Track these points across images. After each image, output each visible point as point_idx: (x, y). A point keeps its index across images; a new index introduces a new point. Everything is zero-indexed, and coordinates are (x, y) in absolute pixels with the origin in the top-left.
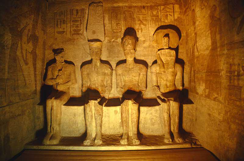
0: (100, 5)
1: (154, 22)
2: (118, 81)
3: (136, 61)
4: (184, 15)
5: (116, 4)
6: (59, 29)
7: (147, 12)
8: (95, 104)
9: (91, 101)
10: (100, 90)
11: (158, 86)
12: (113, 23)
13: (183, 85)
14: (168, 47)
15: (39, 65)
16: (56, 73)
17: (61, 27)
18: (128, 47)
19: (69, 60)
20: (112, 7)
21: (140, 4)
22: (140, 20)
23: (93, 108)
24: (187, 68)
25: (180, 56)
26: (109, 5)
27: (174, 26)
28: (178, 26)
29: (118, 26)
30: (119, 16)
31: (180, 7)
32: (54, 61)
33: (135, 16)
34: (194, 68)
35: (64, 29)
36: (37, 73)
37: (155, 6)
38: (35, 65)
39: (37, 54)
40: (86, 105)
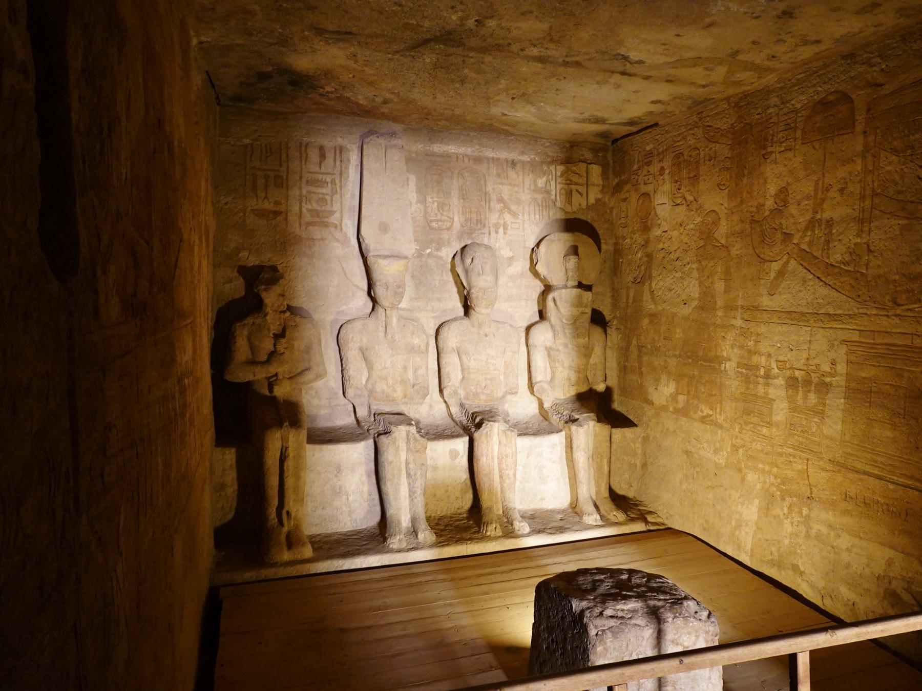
0: (395, 146)
1: (537, 208)
2: (447, 370)
4: (613, 194)
7: (521, 178)
8: (407, 435)
9: (400, 427)
12: (430, 200)
14: (576, 283)
18: (482, 277)
22: (501, 200)
23: (403, 445)
28: (595, 225)
31: (605, 175)
33: (489, 188)
34: (638, 339)
37: (542, 163)
40: (383, 439)
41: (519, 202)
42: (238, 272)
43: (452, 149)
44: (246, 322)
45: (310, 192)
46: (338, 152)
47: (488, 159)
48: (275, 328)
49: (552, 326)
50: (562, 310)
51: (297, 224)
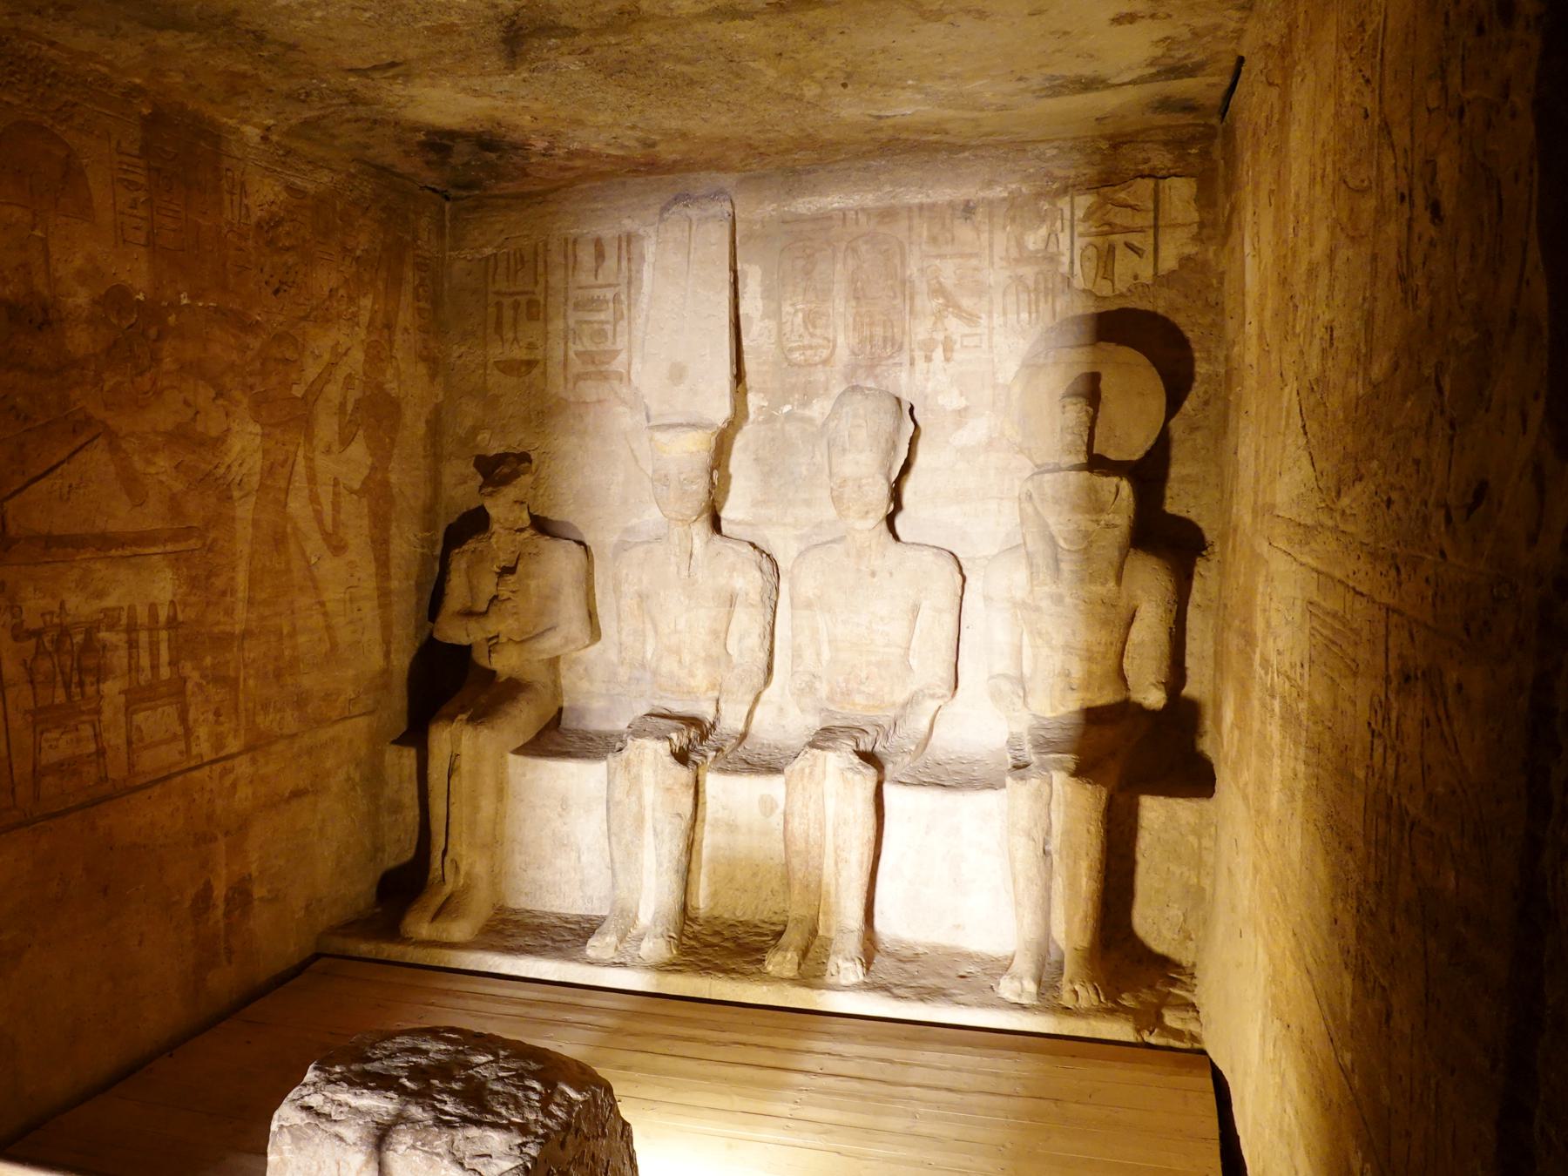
1: (1024, 297)
5: (807, 199)
6: (507, 346)
7: (985, 236)
11: (1021, 681)
12: (791, 310)
15: (406, 543)
16: (488, 586)
17: (516, 339)
20: (788, 218)
22: (939, 291)
27: (1152, 316)
29: (815, 327)
33: (913, 270)
35: (531, 347)
36: (394, 584)
39: (395, 490)
41: (980, 290)
42: (476, 465)
43: (834, 201)
44: (465, 547)
45: (579, 322)
46: (624, 245)
47: (910, 209)
48: (504, 559)
49: (1029, 555)
50: (1051, 520)
51: (561, 381)
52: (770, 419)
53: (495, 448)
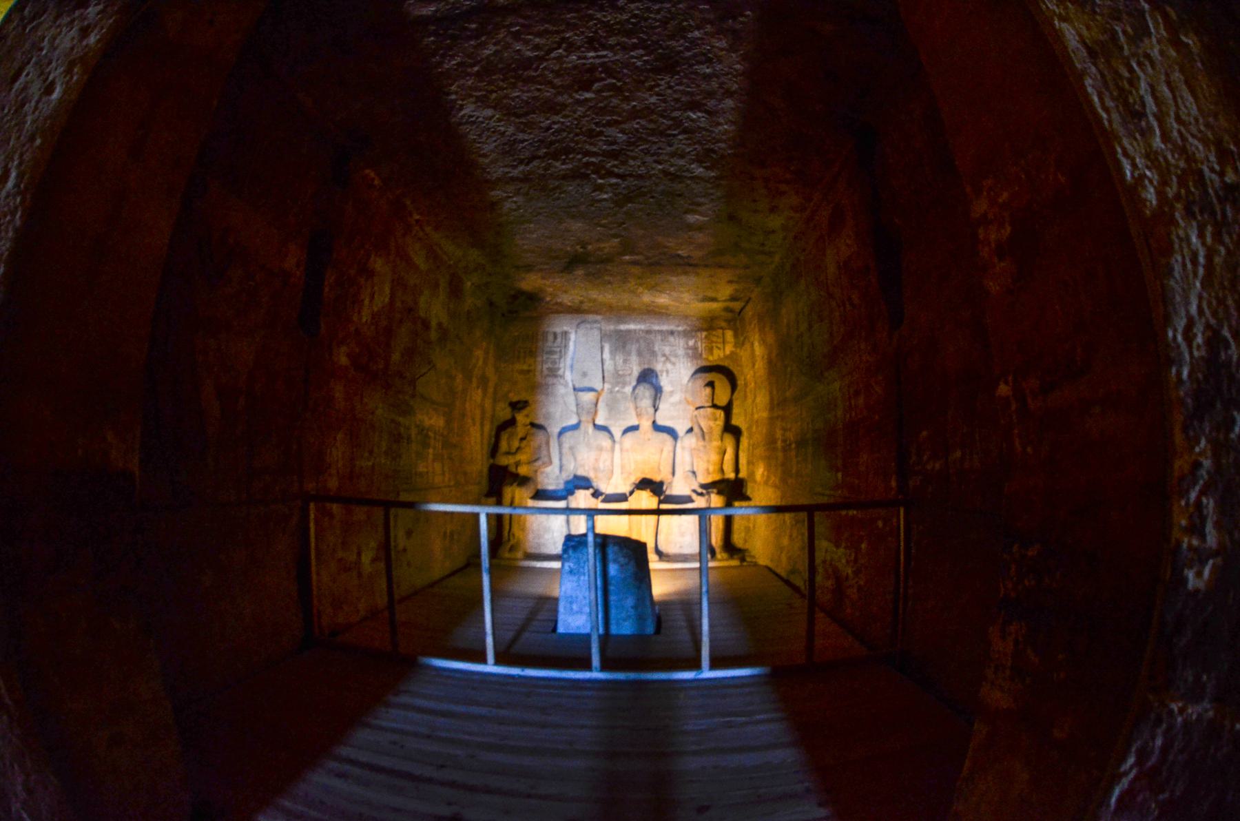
3: (657, 428)
10: (591, 475)
11: (694, 473)
13: (737, 470)
15: (487, 428)
19: (537, 422)
21: (665, 328)
22: (664, 355)
24: (744, 441)
25: (736, 421)
26: (612, 327)
30: (628, 346)
31: (736, 336)
32: (512, 422)
33: (656, 348)
38: (482, 425)
41: (676, 356)
43: (632, 327)
52: (611, 392)
53: (515, 399)
